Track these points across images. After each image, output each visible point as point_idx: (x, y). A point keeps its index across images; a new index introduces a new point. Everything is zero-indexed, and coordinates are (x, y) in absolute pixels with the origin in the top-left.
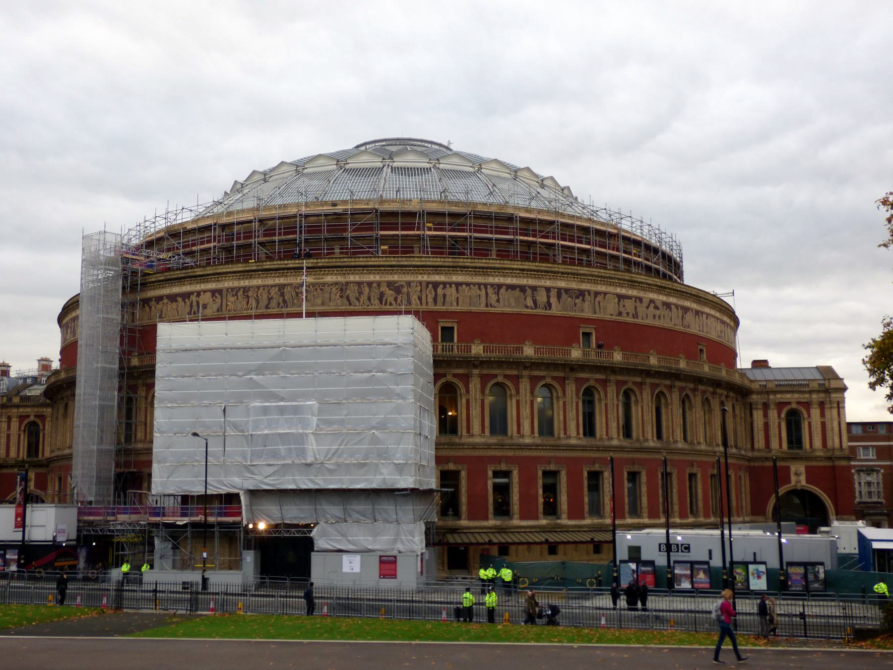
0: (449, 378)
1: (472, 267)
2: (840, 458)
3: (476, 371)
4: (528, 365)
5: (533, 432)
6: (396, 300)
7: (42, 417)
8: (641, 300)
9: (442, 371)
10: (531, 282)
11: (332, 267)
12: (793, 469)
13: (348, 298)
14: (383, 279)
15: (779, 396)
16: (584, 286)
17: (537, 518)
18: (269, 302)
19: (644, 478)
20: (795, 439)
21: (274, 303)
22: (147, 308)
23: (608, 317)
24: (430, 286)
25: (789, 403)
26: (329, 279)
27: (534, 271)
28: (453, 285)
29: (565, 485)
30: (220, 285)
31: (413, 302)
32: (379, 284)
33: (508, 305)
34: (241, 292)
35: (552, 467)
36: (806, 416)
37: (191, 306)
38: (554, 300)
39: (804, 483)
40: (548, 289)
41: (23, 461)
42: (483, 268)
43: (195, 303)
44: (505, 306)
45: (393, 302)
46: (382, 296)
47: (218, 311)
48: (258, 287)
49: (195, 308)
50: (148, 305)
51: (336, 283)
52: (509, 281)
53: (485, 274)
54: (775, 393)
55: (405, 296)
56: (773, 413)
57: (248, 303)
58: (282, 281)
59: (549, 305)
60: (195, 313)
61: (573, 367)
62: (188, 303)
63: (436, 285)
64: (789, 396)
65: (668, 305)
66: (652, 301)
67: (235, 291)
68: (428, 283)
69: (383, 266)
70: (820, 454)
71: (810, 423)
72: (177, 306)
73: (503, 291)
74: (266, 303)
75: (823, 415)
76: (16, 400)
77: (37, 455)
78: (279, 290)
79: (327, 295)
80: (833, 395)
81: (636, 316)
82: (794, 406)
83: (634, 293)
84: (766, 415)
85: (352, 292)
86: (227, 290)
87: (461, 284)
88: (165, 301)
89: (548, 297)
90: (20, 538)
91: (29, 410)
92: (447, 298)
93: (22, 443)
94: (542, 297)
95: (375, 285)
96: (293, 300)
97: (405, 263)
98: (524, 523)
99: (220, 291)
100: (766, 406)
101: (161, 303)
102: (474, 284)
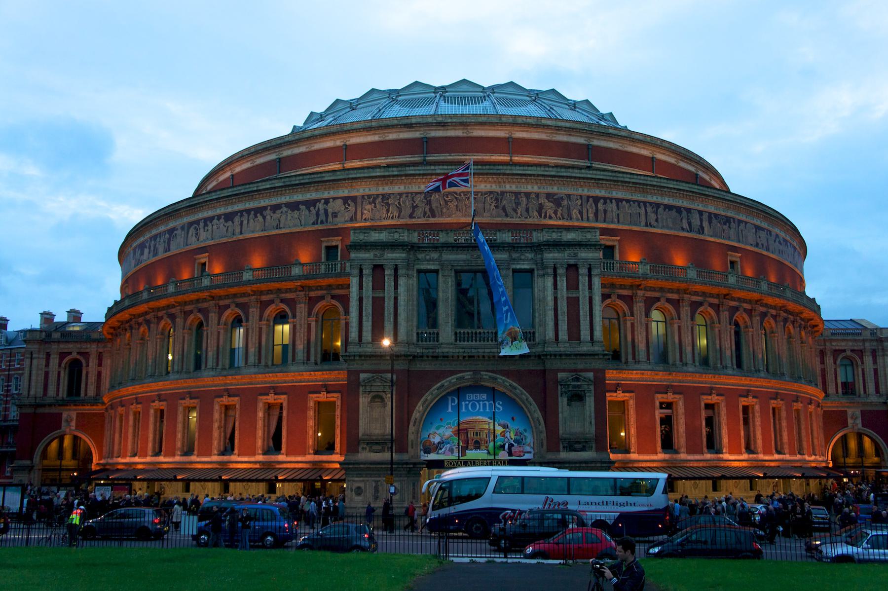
1: (633, 183)
3: (640, 293)
5: (694, 361)
6: (555, 213)
7: (86, 355)
8: (770, 232)
9: (607, 291)
11: (487, 174)
13: (504, 209)
14: (541, 190)
15: (834, 344)
19: (784, 414)
21: (419, 212)
22: (260, 218)
24: (591, 200)
25: (844, 351)
26: (483, 187)
27: (687, 191)
28: (614, 201)
29: (725, 418)
31: (574, 216)
32: (537, 195)
34: (380, 199)
35: (713, 399)
36: (859, 363)
37: (318, 214)
38: (706, 224)
39: (860, 426)
40: (701, 213)
41: (63, 400)
42: (644, 184)
43: (322, 212)
44: (663, 227)
45: (553, 215)
46: (541, 207)
48: (401, 194)
49: (322, 217)
50: (262, 215)
51: (491, 193)
52: (666, 201)
53: (644, 192)
54: (831, 341)
55: (565, 210)
56: (829, 360)
57: (388, 211)
59: (701, 230)
62: (314, 212)
63: (596, 199)
64: (843, 344)
65: (785, 240)
66: (777, 236)
67: (372, 199)
68: (588, 197)
69: (543, 176)
70: (874, 399)
71: (863, 370)
73: (661, 210)
74: (409, 211)
76: (56, 336)
77: (78, 394)
78: (425, 198)
79: (480, 205)
82: (849, 353)
83: (764, 225)
84: (822, 362)
86: (363, 197)
87: (621, 200)
88: (284, 209)
89: (701, 221)
91: (71, 346)
92: (608, 214)
93: (61, 381)
94: (696, 222)
95: (533, 196)
96: (442, 209)
97: (565, 174)
98: (690, 457)
99: (354, 199)
100: (822, 354)
101: (279, 211)
102: (634, 201)
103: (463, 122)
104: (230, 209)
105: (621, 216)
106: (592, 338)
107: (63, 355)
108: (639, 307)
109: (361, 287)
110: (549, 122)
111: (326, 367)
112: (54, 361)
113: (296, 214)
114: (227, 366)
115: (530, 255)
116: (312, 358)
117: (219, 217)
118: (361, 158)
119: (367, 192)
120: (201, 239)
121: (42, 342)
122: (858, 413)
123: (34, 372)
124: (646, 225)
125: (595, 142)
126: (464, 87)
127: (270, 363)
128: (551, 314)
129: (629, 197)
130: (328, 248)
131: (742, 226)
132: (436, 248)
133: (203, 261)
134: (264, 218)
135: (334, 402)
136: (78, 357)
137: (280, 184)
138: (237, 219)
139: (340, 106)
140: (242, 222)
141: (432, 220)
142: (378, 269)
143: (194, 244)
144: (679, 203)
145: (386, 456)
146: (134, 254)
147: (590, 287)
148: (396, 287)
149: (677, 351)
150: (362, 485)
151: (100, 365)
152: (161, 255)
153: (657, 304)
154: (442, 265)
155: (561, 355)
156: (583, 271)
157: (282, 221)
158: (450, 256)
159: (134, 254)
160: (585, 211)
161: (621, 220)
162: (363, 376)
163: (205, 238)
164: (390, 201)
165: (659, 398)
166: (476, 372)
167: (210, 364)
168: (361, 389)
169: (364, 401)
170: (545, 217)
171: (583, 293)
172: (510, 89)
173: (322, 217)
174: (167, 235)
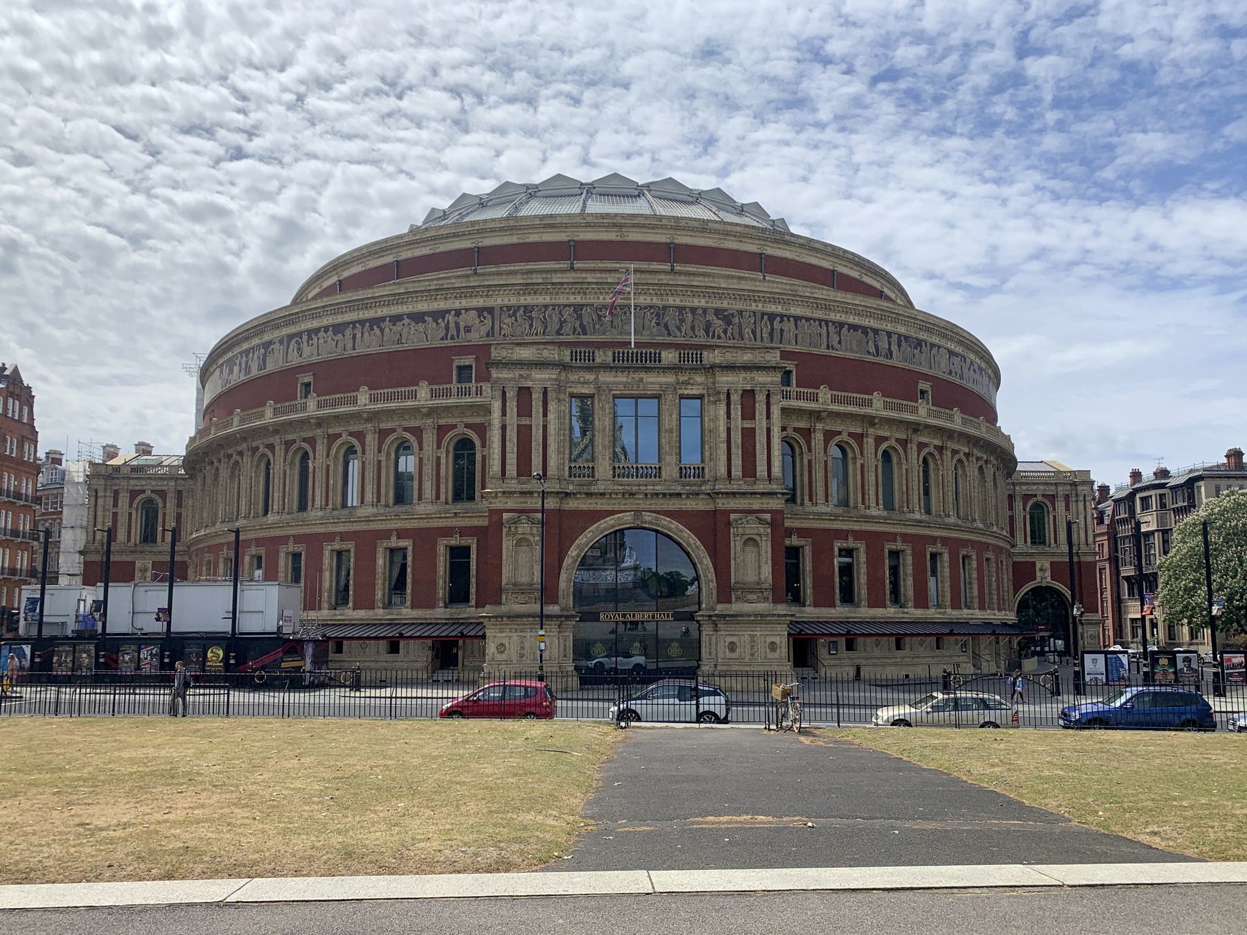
0: (790, 431)
2: (1085, 554)
3: (819, 426)
4: (876, 421)
6: (725, 332)
10: (873, 323)
12: (1038, 566)
13: (666, 326)
15: (1024, 487)
16: (923, 336)
17: (885, 607)
18: (561, 327)
20: (1038, 537)
21: (567, 328)
23: (941, 375)
25: (1035, 496)
26: (642, 300)
30: (490, 302)
32: (705, 310)
33: (849, 349)
35: (899, 545)
36: (1051, 509)
37: (447, 328)
38: (894, 348)
39: (1049, 579)
40: (889, 334)
43: (452, 325)
45: (722, 335)
46: (708, 326)
47: (488, 335)
48: (546, 307)
49: (453, 331)
50: (379, 327)
51: (651, 307)
52: (852, 319)
56: (1018, 505)
57: (531, 326)
58: (579, 299)
59: (890, 354)
60: (453, 338)
61: (916, 428)
63: (772, 317)
65: (979, 368)
66: (972, 363)
67: (512, 310)
68: (763, 314)
72: (426, 329)
75: (1067, 508)
80: (1079, 488)
81: (961, 378)
82: (1040, 498)
83: (959, 349)
84: (1011, 508)
85: (671, 319)
88: (406, 321)
89: (890, 344)
90: (229, 629)
91: (144, 482)
93: (133, 524)
94: (884, 345)
99: (490, 310)
100: (1011, 498)
102: (814, 320)
103: (614, 222)
104: (339, 319)
105: (800, 337)
106: (769, 475)
107: (134, 494)
108: (818, 437)
109: (504, 414)
110: (716, 226)
111: (459, 507)
112: (124, 499)
113: (421, 327)
114: (339, 506)
115: (699, 379)
116: (443, 496)
117: (326, 329)
118: (496, 263)
119: (506, 302)
120: (304, 355)
121: (109, 477)
122: (1047, 565)
123: (100, 513)
124: (828, 348)
125: (770, 251)
126: (614, 182)
127: (391, 502)
128: (724, 446)
129: (809, 314)
130: (460, 368)
131: (935, 350)
132: (590, 369)
133: (306, 380)
134: (382, 330)
135: (467, 549)
136: (153, 496)
137: (402, 291)
138: (348, 332)
139: (467, 202)
140: (355, 335)
141: (583, 338)
142: (524, 393)
143: (295, 360)
144: (866, 322)
145: (536, 608)
146: (221, 372)
147: (768, 417)
148: (545, 415)
149: (860, 491)
150: (506, 642)
151: (179, 505)
152: (255, 372)
153: (838, 438)
154: (598, 388)
155: (734, 494)
156: (761, 398)
157: (405, 335)
158: (606, 378)
159: (221, 372)
160: (758, 330)
161: (800, 340)
162: (505, 516)
163: (310, 354)
164: (534, 314)
165: (837, 545)
166: (638, 513)
167: (318, 503)
168: (505, 530)
169: (507, 544)
170: (713, 337)
171: (760, 423)
172: (670, 187)
173: (453, 331)
174: (262, 351)
